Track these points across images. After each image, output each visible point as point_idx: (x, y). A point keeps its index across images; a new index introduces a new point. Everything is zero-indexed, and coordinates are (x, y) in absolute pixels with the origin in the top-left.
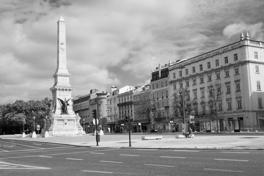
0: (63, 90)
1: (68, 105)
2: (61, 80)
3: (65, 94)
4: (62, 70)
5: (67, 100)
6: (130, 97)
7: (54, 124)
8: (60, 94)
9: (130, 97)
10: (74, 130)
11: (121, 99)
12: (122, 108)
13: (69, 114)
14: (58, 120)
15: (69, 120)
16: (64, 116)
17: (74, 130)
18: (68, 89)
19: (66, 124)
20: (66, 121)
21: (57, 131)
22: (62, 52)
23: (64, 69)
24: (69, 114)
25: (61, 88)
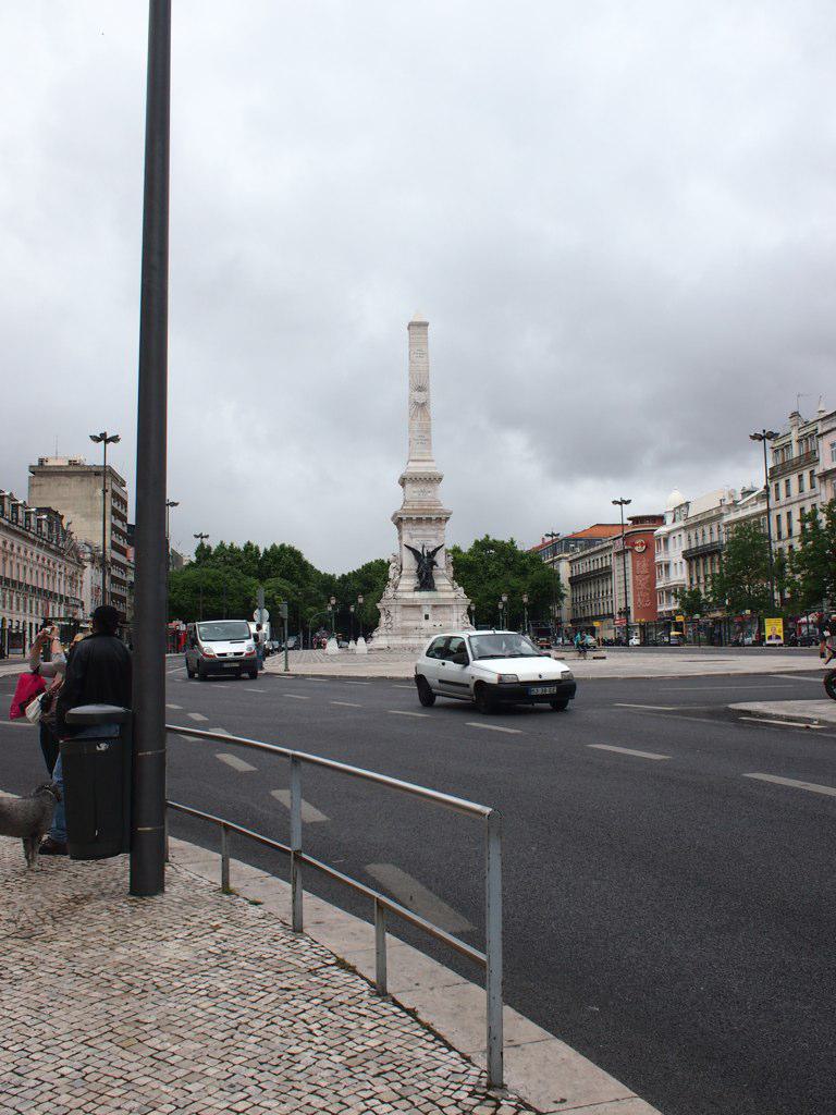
0: (419, 520)
1: (435, 563)
4: (421, 464)
5: (431, 550)
6: (715, 529)
8: (413, 533)
9: (715, 529)
11: (693, 536)
12: (697, 565)
13: (436, 590)
14: (404, 606)
15: (435, 606)
16: (425, 594)
18: (434, 517)
19: (427, 617)
20: (427, 611)
24: (436, 590)
25: (414, 517)
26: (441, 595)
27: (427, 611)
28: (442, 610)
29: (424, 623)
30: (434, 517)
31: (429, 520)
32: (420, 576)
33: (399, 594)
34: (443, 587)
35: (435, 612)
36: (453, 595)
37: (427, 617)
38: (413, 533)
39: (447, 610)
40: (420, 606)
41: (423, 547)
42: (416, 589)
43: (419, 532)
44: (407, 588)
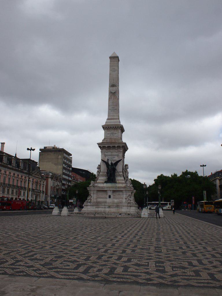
2: (108, 134)
3: (113, 154)
4: (112, 121)
5: (113, 162)
7: (91, 196)
8: (106, 153)
10: (121, 206)
14: (98, 191)
15: (114, 191)
16: (109, 185)
17: (121, 206)
19: (110, 197)
21: (95, 207)
22: (112, 98)
23: (113, 119)
25: (106, 146)
26: (118, 185)
27: (110, 193)
28: (118, 193)
29: (108, 200)
30: (116, 145)
31: (114, 147)
32: (108, 176)
33: (96, 185)
34: (120, 181)
35: (114, 194)
36: (124, 185)
37: (110, 197)
38: (106, 153)
39: (121, 193)
40: (106, 191)
41: (108, 159)
42: (106, 182)
43: (109, 153)
44: (102, 181)
